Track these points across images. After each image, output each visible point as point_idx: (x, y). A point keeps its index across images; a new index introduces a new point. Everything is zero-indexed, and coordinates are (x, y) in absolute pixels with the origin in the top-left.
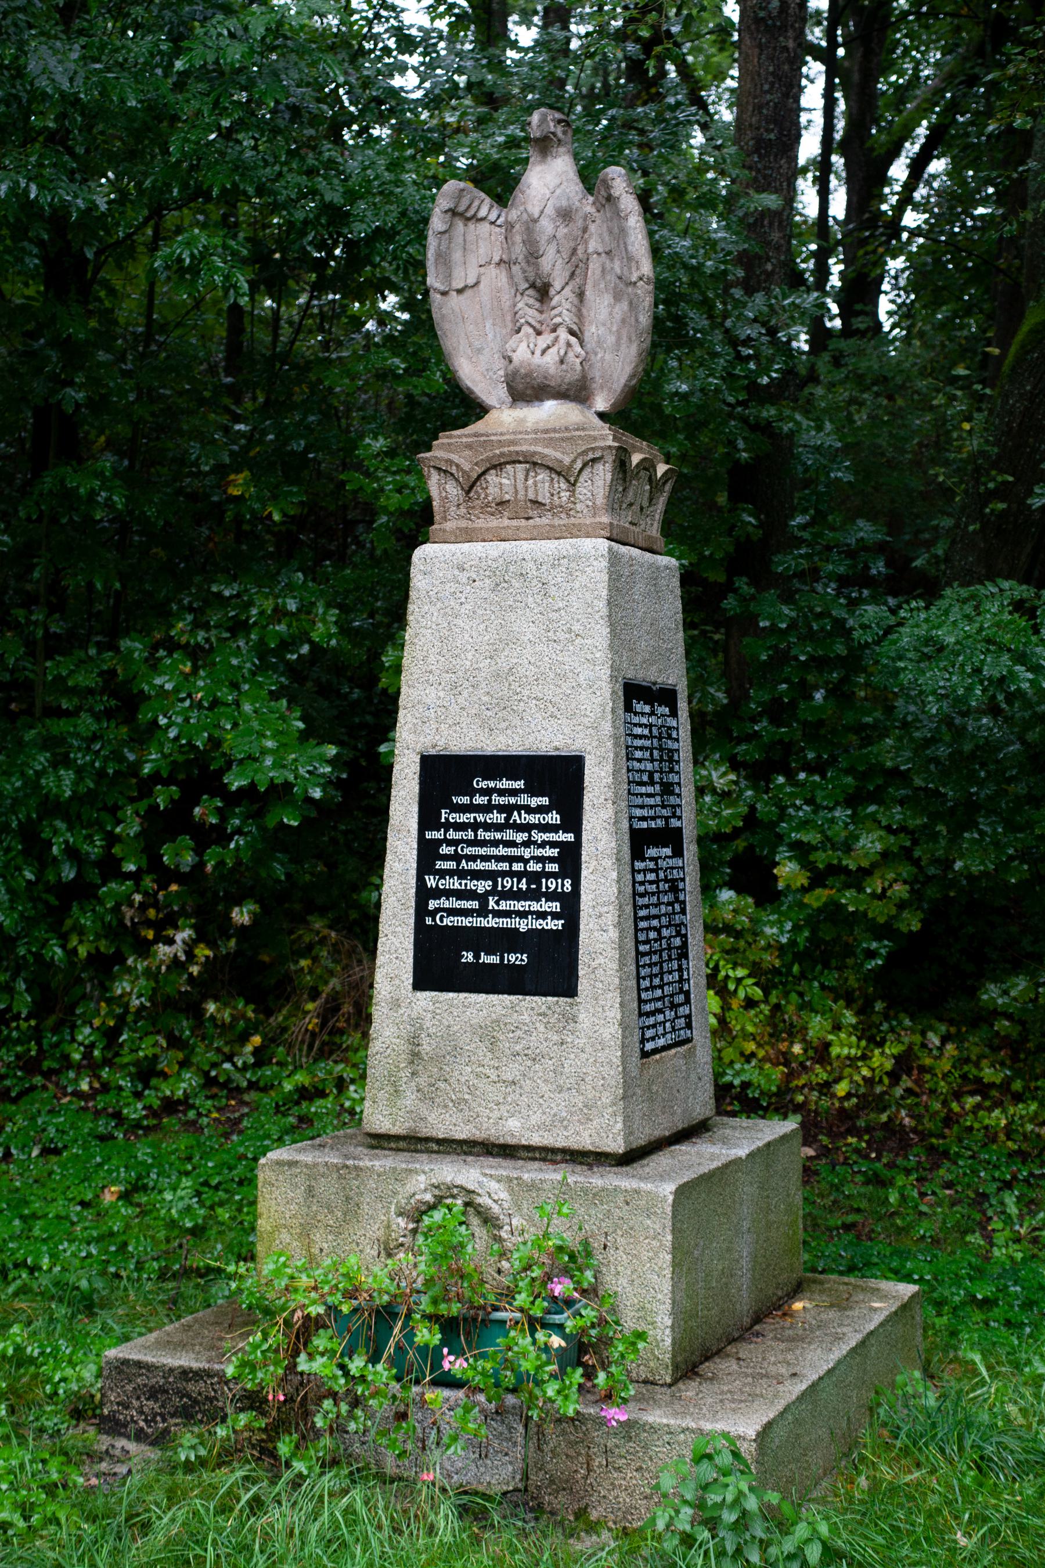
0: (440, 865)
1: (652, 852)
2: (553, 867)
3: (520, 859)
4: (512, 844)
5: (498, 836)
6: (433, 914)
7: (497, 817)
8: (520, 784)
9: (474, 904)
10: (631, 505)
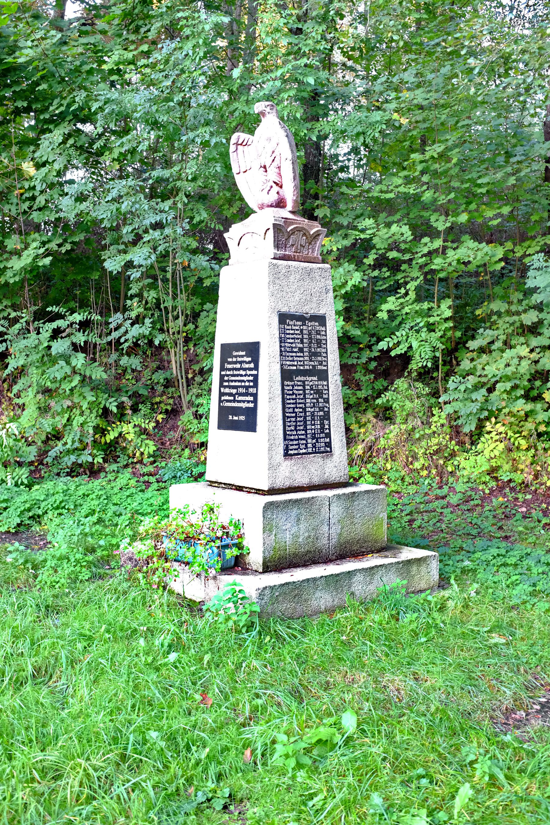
1: (299, 378)
2: (251, 384)
3: (243, 381)
4: (241, 375)
6: (222, 402)
7: (238, 366)
8: (244, 353)
9: (232, 398)
10: (293, 245)
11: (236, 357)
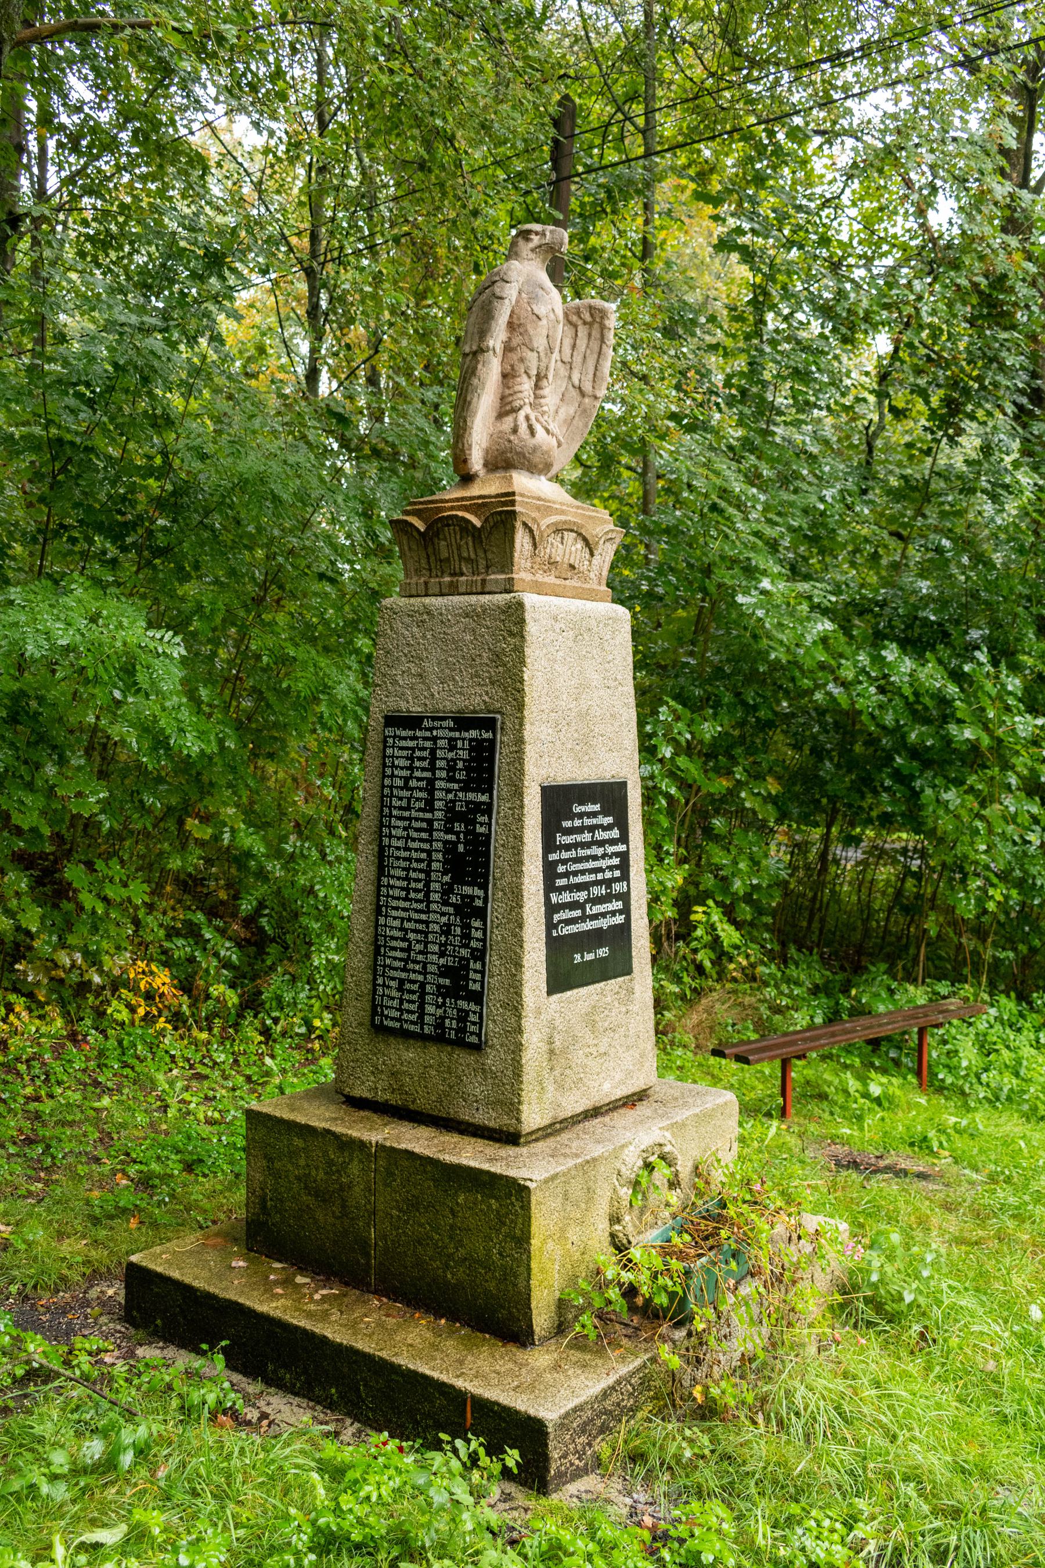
0: (561, 882)
2: (617, 873)
4: (595, 858)
5: (588, 852)
6: (555, 926)
7: (587, 837)
8: (597, 807)
11: (581, 816)
